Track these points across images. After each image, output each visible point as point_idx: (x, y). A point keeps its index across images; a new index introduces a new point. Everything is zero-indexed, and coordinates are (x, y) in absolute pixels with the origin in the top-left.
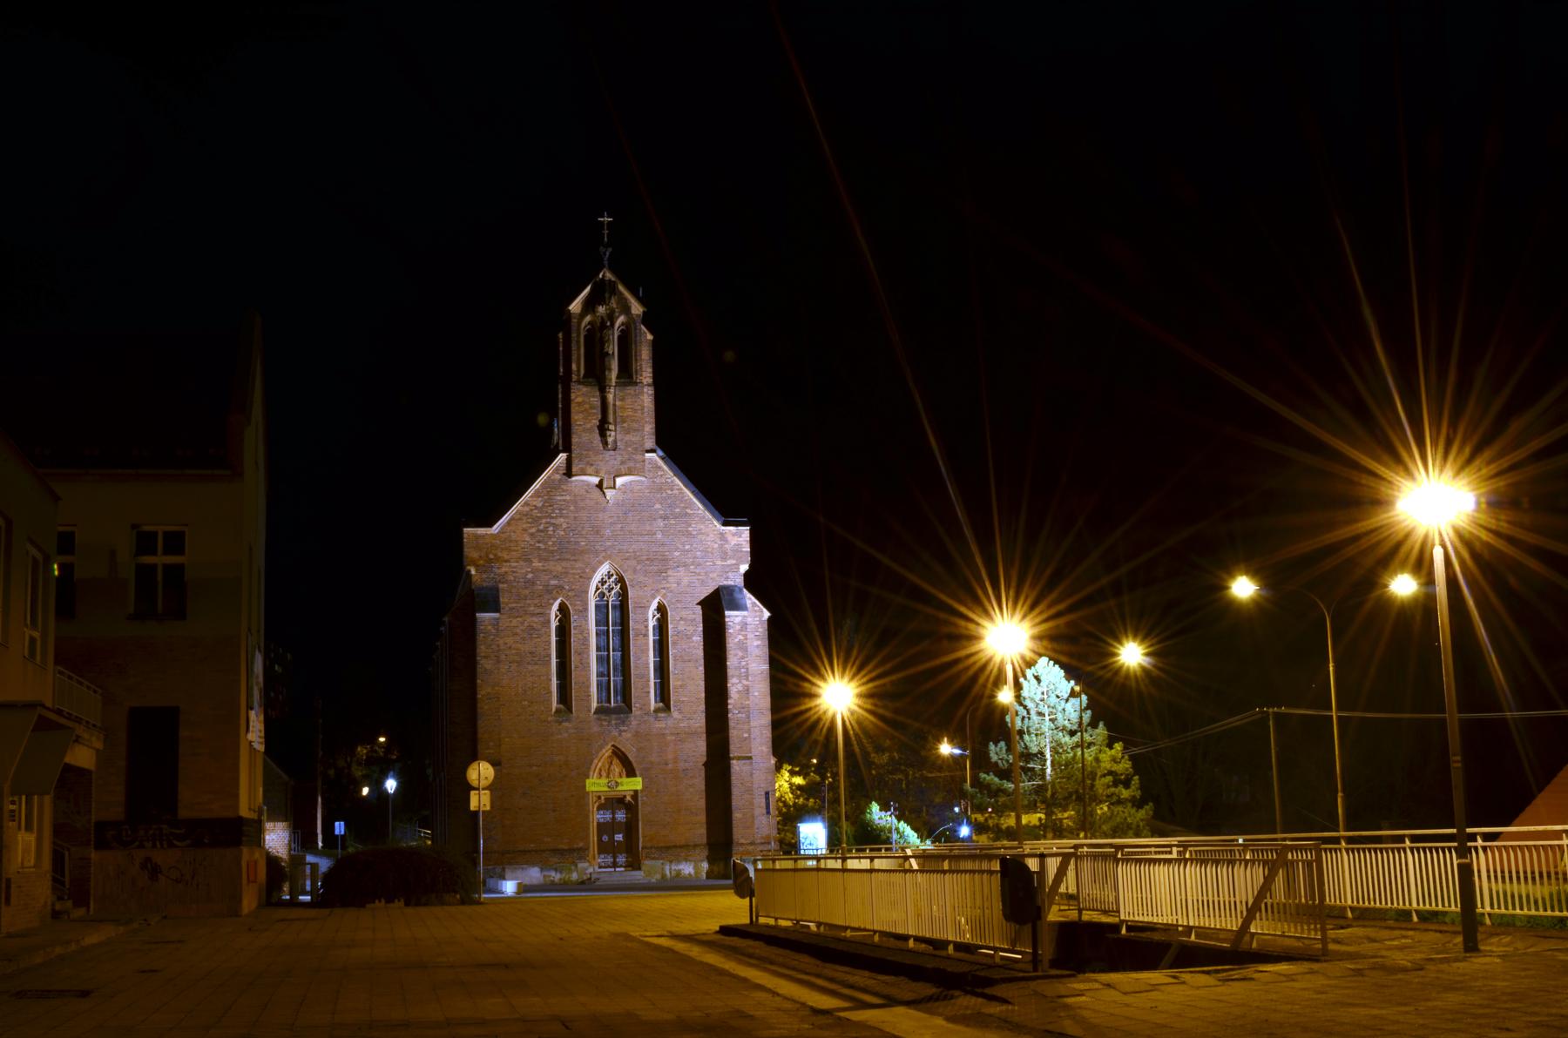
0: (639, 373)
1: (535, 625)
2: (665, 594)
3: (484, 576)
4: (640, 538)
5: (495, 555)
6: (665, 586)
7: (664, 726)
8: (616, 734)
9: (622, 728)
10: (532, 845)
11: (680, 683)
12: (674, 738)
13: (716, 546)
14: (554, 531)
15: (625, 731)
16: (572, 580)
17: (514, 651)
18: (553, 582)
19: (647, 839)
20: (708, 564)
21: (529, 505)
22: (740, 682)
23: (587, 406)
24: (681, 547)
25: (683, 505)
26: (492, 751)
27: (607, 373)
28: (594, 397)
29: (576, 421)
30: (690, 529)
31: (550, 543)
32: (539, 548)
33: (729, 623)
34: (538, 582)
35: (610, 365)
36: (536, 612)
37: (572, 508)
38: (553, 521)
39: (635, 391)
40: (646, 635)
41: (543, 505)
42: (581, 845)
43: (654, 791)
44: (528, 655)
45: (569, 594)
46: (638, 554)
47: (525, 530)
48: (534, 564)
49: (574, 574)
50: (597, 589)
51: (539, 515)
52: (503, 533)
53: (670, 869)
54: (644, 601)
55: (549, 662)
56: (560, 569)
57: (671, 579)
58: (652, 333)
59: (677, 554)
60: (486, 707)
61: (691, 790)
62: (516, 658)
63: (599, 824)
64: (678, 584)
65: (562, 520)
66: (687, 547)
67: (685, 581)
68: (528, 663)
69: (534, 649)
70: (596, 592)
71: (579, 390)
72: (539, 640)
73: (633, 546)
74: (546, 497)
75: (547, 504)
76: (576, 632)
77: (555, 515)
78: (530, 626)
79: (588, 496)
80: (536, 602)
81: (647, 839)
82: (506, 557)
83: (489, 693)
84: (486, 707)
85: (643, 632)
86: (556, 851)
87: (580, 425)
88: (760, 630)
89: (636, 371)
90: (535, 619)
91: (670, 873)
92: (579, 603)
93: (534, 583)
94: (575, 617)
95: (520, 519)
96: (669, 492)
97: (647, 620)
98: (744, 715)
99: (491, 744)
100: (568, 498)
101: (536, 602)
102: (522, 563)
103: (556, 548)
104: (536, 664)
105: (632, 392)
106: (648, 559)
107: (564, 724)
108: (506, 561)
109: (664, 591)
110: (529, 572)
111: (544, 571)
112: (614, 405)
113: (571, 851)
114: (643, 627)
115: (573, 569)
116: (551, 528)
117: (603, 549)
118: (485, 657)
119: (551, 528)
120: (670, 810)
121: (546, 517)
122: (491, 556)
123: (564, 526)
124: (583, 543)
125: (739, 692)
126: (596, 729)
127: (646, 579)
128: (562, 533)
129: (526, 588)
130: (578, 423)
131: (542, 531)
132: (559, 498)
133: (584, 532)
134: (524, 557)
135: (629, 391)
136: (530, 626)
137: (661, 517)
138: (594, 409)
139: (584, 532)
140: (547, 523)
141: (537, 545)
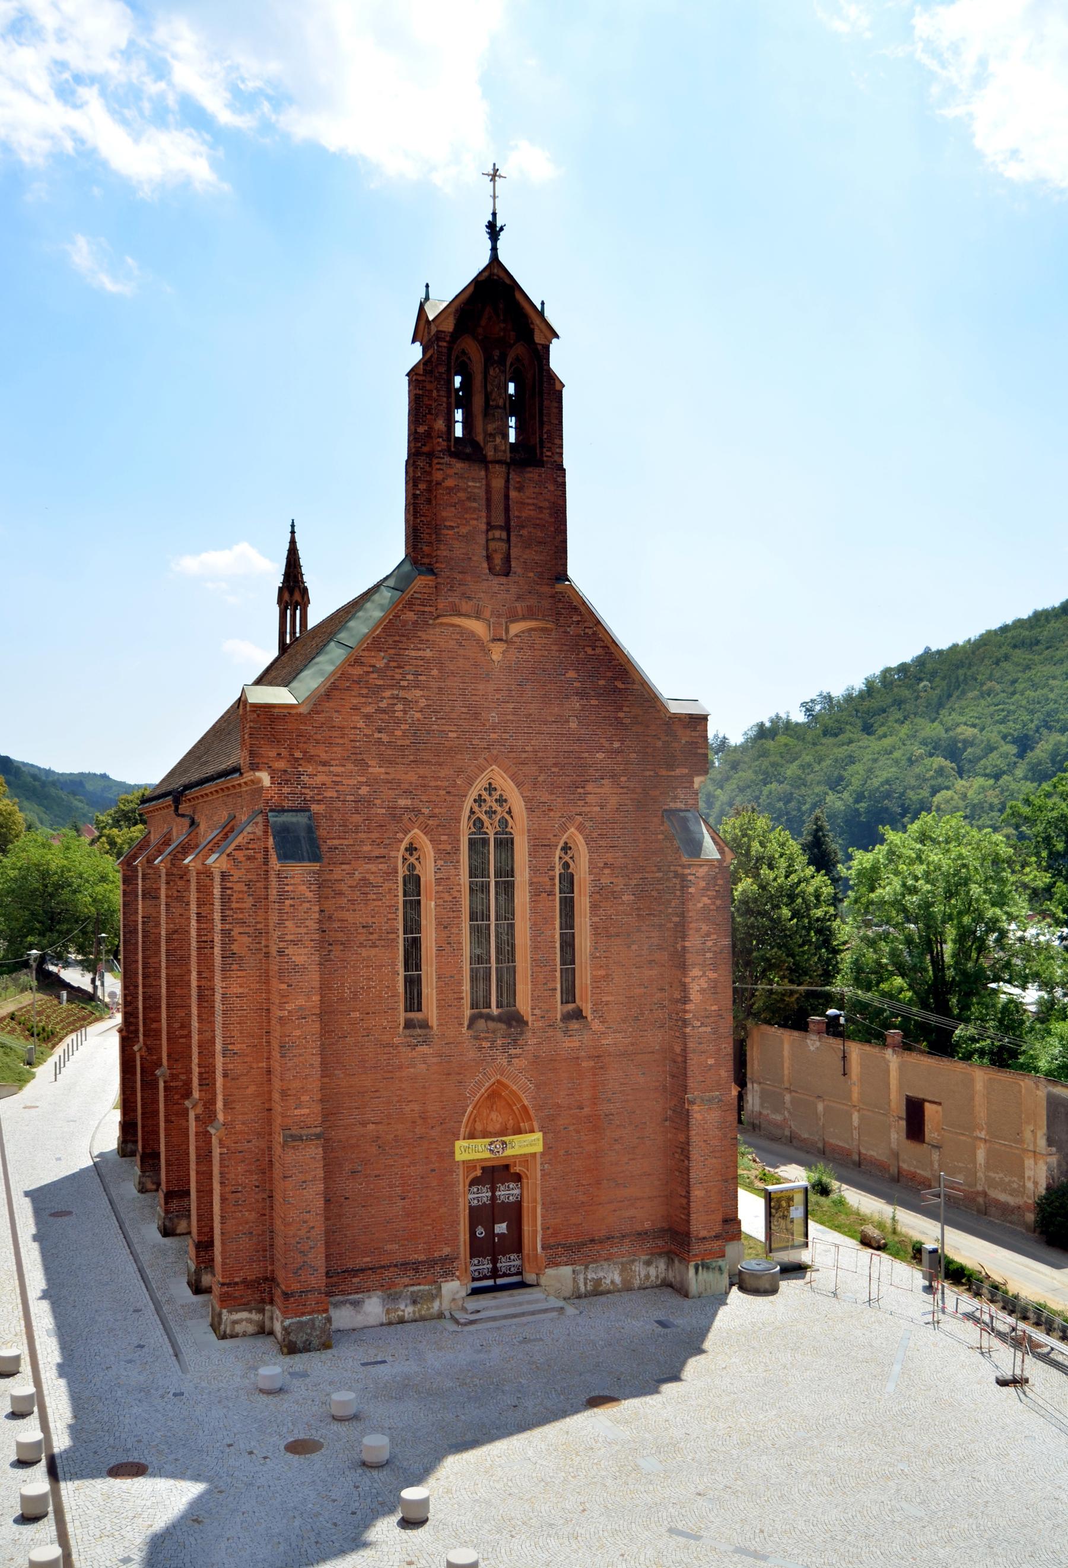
1: (371, 878)
3: (286, 790)
4: (544, 728)
5: (305, 752)
7: (577, 1044)
9: (512, 1051)
10: (368, 1259)
11: (602, 972)
12: (592, 1063)
13: (659, 744)
14: (405, 712)
15: (517, 1056)
16: (434, 798)
17: (336, 925)
18: (402, 802)
19: (549, 1232)
20: (648, 773)
21: (362, 664)
22: (704, 974)
23: (462, 495)
24: (606, 744)
25: (609, 674)
26: (306, 1111)
28: (474, 480)
30: (621, 715)
31: (398, 733)
32: (379, 741)
33: (690, 878)
34: (378, 802)
36: (376, 853)
37: (435, 672)
38: (402, 694)
41: (387, 666)
42: (447, 1250)
43: (562, 1153)
44: (361, 930)
45: (430, 822)
46: (540, 755)
47: (355, 708)
48: (371, 770)
49: (438, 788)
50: (472, 812)
51: (381, 682)
53: (586, 1279)
54: (550, 836)
56: (412, 777)
57: (590, 799)
59: (600, 756)
60: (297, 1033)
61: (617, 1147)
62: (341, 937)
63: (471, 1208)
64: (602, 807)
65: (419, 693)
66: (616, 745)
67: (613, 801)
68: (361, 946)
69: (370, 920)
70: (469, 817)
73: (533, 743)
74: (392, 651)
75: (393, 664)
77: (403, 683)
78: (364, 879)
79: (461, 652)
80: (374, 835)
81: (549, 1232)
82: (324, 756)
83: (301, 1008)
84: (297, 1033)
85: (548, 888)
86: (407, 1266)
87: (452, 528)
88: (720, 882)
90: (373, 867)
91: (585, 1284)
93: (369, 803)
94: (442, 862)
95: (348, 689)
96: (589, 651)
98: (709, 1029)
99: (305, 1098)
100: (428, 653)
101: (374, 835)
102: (350, 766)
103: (408, 742)
105: (536, 477)
106: (555, 765)
107: (419, 1048)
108: (324, 764)
109: (579, 818)
110: (361, 783)
112: (507, 497)
113: (431, 1263)
114: (547, 879)
115: (437, 778)
116: (400, 707)
117: (485, 745)
118: (294, 943)
119: (400, 707)
120: (584, 1182)
121: (392, 687)
122: (298, 754)
123: (423, 703)
124: (451, 735)
125: (702, 991)
126: (472, 1054)
127: (553, 797)
128: (418, 715)
130: (448, 524)
131: (384, 711)
132: (413, 653)
133: (454, 715)
134: (353, 757)
135: (531, 475)
136: (364, 879)
137: (577, 694)
138: (475, 500)
139: (454, 715)
140: (393, 697)
141: (377, 735)
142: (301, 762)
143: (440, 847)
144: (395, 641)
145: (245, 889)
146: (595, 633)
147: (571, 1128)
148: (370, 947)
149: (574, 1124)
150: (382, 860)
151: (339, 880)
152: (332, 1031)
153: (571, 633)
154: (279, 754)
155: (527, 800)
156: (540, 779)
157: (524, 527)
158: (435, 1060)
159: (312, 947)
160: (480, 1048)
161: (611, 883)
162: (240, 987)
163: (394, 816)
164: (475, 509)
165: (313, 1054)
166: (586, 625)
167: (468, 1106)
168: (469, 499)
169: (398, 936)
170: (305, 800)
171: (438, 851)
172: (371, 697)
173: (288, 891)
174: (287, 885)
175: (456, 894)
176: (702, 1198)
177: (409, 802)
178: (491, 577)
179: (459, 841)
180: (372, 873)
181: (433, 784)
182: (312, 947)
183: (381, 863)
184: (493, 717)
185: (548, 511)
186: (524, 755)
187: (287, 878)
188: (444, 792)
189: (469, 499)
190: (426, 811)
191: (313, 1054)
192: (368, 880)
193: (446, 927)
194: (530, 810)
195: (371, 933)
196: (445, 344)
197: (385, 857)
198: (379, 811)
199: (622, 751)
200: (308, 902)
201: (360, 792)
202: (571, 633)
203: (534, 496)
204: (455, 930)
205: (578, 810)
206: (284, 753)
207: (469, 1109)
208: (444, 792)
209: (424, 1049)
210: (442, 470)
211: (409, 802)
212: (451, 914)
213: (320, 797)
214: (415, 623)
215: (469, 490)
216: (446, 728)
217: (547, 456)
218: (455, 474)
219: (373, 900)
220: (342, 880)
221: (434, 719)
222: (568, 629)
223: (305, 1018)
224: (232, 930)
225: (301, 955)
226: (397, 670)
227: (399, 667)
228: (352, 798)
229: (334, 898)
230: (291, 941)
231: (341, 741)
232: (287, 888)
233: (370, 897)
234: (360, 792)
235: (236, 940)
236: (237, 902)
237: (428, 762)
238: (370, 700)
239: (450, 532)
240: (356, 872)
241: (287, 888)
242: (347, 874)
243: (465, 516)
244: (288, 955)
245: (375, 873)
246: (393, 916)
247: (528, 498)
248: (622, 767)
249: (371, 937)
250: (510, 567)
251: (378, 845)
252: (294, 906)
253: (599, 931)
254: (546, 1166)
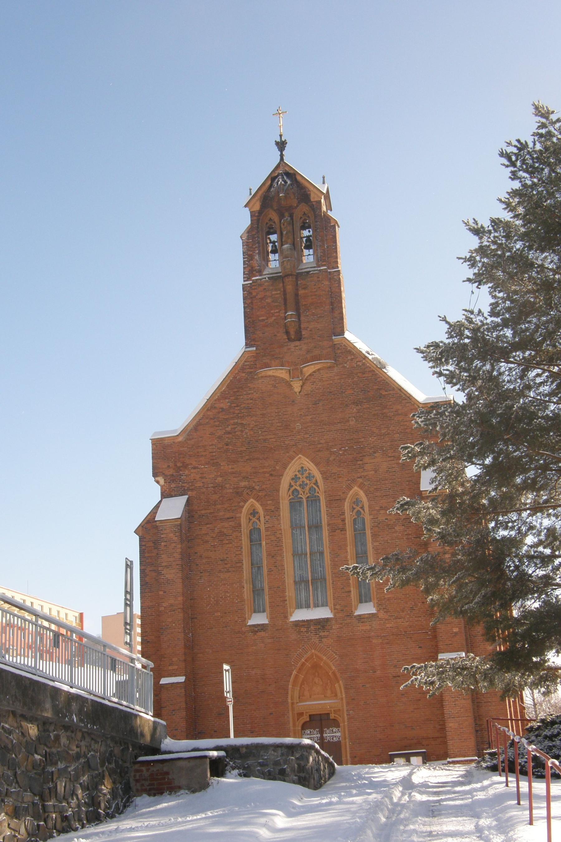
1: (225, 531)
2: (362, 483)
3: (173, 485)
5: (183, 463)
6: (363, 474)
7: (368, 627)
8: (317, 641)
9: (322, 634)
18: (243, 484)
25: (377, 387)
26: (176, 667)
34: (227, 486)
36: (228, 515)
40: (343, 530)
41: (230, 407)
45: (260, 494)
46: (330, 444)
49: (264, 473)
50: (291, 486)
52: (190, 440)
54: (340, 493)
55: (239, 569)
60: (170, 620)
68: (220, 571)
72: (231, 545)
74: (233, 398)
75: (233, 405)
76: (269, 533)
78: (221, 532)
83: (172, 605)
84: (170, 620)
85: (340, 526)
87: (263, 320)
90: (226, 524)
92: (269, 502)
94: (267, 517)
97: (343, 514)
99: (174, 659)
103: (244, 449)
104: (228, 571)
107: (259, 634)
109: (360, 480)
111: (233, 473)
112: (297, 295)
116: (239, 428)
118: (167, 567)
122: (179, 464)
129: (215, 493)
130: (261, 318)
131: (229, 433)
134: (211, 462)
136: (221, 532)
137: (354, 403)
142: (181, 468)
143: (267, 508)
144: (234, 392)
145: (152, 545)
146: (364, 364)
147: (368, 686)
148: (226, 572)
149: (369, 683)
150: (231, 520)
151: (206, 534)
152: (204, 625)
153: (348, 367)
154: (169, 466)
155: (322, 473)
156: (331, 459)
158: (270, 641)
159: (177, 569)
160: (300, 632)
161: (387, 519)
162: (151, 602)
163: (237, 493)
165: (179, 632)
166: (357, 360)
167: (293, 670)
169: (243, 564)
170: (184, 490)
171: (265, 510)
172: (221, 426)
173: (163, 538)
174: (162, 534)
175: (278, 536)
176: (455, 729)
177: (247, 483)
179: (279, 503)
180: (226, 528)
181: (261, 471)
182: (177, 569)
183: (231, 521)
184: (298, 426)
186: (319, 446)
187: (162, 530)
188: (268, 475)
189: (273, 301)
190: (257, 488)
191: (179, 632)
192: (223, 532)
193: (272, 557)
194: (325, 479)
195: (226, 564)
197: (233, 518)
198: (228, 491)
199: (388, 434)
200: (174, 543)
201: (217, 481)
202: (348, 367)
204: (279, 558)
205: (359, 475)
206: (171, 464)
207: (294, 672)
208: (268, 475)
209: (262, 634)
211: (247, 483)
212: (276, 548)
213: (193, 487)
214: (246, 379)
216: (268, 437)
219: (227, 544)
220: (207, 534)
221: (260, 433)
222: (345, 365)
223: (174, 611)
224: (146, 569)
225: (171, 573)
226: (236, 408)
227: (237, 406)
228: (212, 485)
229: (203, 544)
230: (165, 566)
231: (204, 454)
232: (162, 536)
233: (224, 542)
234: (217, 481)
235: (148, 575)
236: (148, 553)
237: (258, 459)
238: (221, 428)
240: (216, 529)
241: (162, 536)
242: (210, 530)
244: (163, 574)
245: (227, 528)
246: (239, 552)
248: (389, 444)
249: (226, 566)
251: (229, 511)
252: (166, 546)
253: (379, 551)
254: (351, 712)
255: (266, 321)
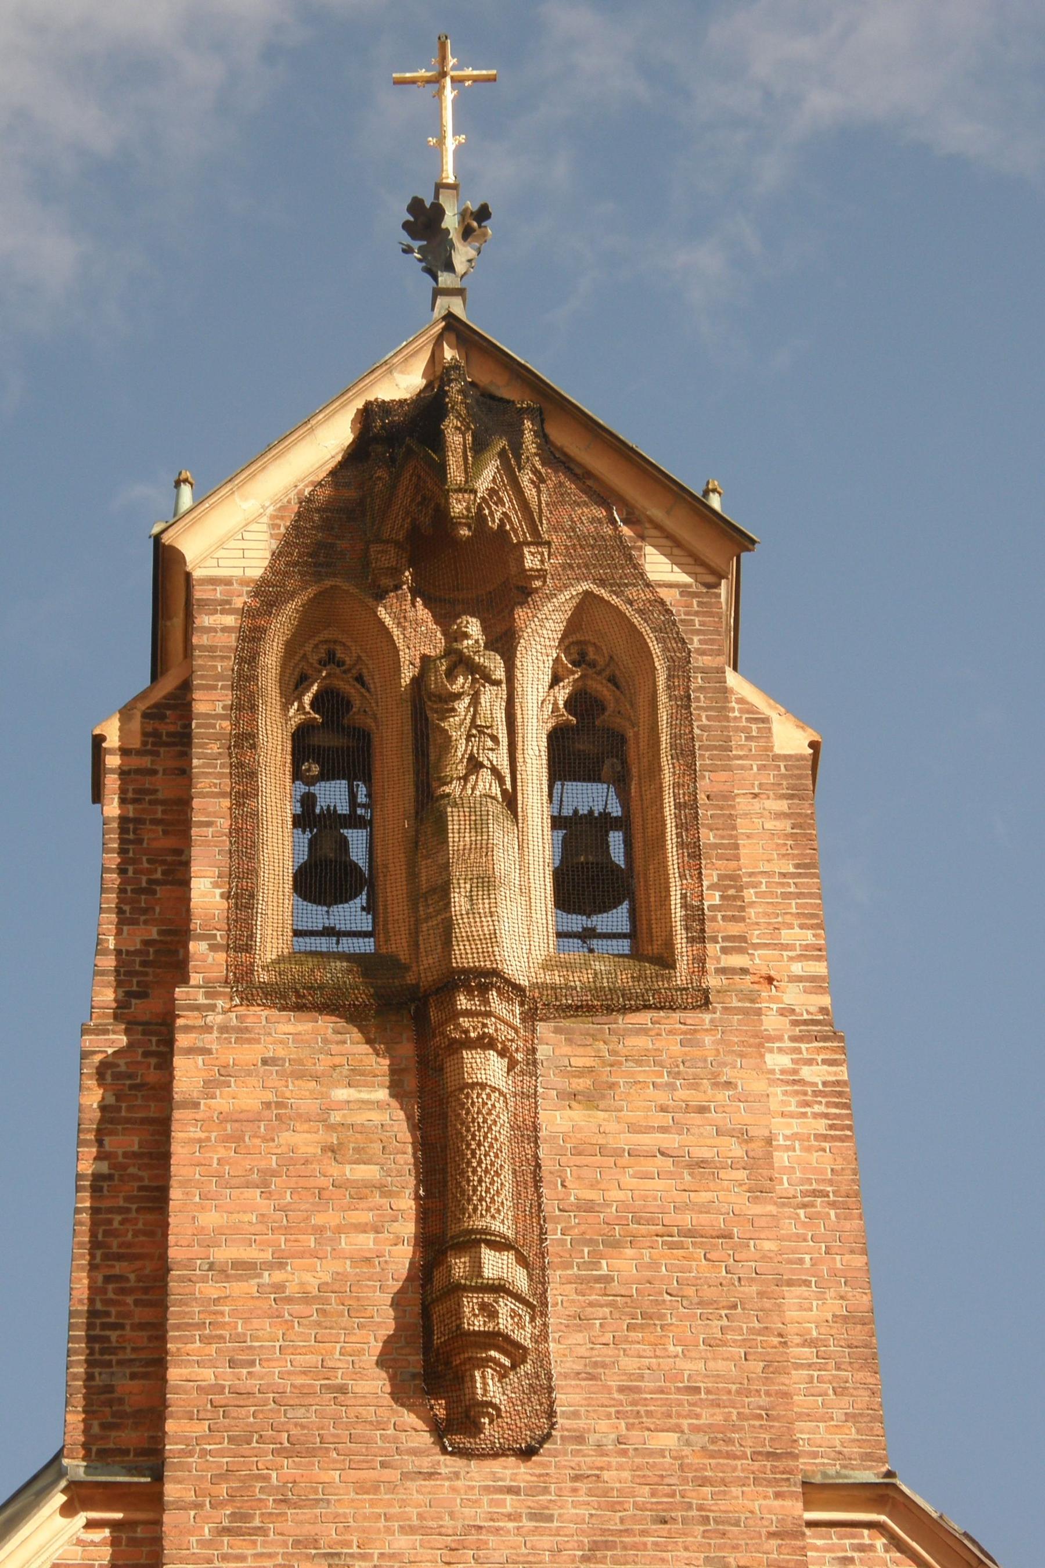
0: (716, 926)
27: (459, 901)
29: (210, 1239)
35: (486, 849)
39: (690, 1039)
58: (802, 717)
71: (242, 1034)
87: (246, 1268)
89: (696, 916)
105: (672, 1047)
130: (223, 1254)
135: (639, 1043)
157: (615, 1244)
164: (360, 1191)
168: (332, 1150)
178: (449, 1464)
185: (742, 1175)
196: (230, 620)
203: (667, 1119)
210: (205, 1051)
215: (336, 1117)
217: (722, 971)
218: (265, 1062)
239: (237, 1288)
243: (317, 1220)
247: (633, 1128)
250: (551, 1414)
255: (266, 1277)
